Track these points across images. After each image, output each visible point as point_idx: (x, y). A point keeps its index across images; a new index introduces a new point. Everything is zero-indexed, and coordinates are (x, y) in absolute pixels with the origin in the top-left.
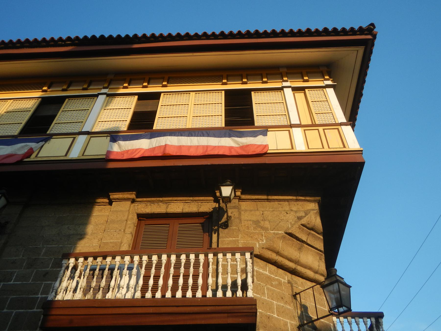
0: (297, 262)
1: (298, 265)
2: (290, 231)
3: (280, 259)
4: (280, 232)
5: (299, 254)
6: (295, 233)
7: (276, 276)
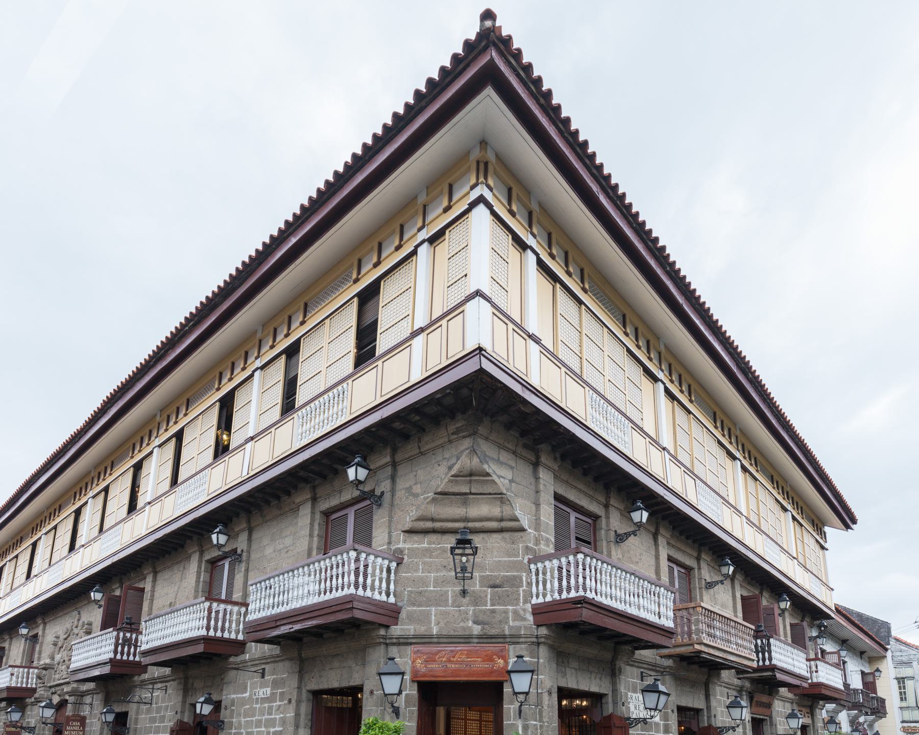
0: (466, 520)
1: (468, 522)
2: (439, 490)
3: (438, 525)
4: (429, 495)
5: (465, 510)
6: (446, 490)
7: (439, 544)
